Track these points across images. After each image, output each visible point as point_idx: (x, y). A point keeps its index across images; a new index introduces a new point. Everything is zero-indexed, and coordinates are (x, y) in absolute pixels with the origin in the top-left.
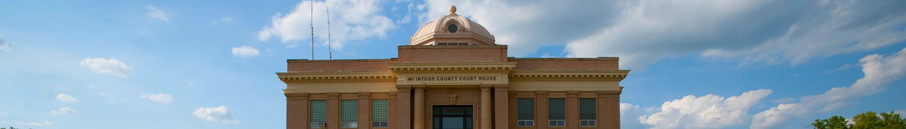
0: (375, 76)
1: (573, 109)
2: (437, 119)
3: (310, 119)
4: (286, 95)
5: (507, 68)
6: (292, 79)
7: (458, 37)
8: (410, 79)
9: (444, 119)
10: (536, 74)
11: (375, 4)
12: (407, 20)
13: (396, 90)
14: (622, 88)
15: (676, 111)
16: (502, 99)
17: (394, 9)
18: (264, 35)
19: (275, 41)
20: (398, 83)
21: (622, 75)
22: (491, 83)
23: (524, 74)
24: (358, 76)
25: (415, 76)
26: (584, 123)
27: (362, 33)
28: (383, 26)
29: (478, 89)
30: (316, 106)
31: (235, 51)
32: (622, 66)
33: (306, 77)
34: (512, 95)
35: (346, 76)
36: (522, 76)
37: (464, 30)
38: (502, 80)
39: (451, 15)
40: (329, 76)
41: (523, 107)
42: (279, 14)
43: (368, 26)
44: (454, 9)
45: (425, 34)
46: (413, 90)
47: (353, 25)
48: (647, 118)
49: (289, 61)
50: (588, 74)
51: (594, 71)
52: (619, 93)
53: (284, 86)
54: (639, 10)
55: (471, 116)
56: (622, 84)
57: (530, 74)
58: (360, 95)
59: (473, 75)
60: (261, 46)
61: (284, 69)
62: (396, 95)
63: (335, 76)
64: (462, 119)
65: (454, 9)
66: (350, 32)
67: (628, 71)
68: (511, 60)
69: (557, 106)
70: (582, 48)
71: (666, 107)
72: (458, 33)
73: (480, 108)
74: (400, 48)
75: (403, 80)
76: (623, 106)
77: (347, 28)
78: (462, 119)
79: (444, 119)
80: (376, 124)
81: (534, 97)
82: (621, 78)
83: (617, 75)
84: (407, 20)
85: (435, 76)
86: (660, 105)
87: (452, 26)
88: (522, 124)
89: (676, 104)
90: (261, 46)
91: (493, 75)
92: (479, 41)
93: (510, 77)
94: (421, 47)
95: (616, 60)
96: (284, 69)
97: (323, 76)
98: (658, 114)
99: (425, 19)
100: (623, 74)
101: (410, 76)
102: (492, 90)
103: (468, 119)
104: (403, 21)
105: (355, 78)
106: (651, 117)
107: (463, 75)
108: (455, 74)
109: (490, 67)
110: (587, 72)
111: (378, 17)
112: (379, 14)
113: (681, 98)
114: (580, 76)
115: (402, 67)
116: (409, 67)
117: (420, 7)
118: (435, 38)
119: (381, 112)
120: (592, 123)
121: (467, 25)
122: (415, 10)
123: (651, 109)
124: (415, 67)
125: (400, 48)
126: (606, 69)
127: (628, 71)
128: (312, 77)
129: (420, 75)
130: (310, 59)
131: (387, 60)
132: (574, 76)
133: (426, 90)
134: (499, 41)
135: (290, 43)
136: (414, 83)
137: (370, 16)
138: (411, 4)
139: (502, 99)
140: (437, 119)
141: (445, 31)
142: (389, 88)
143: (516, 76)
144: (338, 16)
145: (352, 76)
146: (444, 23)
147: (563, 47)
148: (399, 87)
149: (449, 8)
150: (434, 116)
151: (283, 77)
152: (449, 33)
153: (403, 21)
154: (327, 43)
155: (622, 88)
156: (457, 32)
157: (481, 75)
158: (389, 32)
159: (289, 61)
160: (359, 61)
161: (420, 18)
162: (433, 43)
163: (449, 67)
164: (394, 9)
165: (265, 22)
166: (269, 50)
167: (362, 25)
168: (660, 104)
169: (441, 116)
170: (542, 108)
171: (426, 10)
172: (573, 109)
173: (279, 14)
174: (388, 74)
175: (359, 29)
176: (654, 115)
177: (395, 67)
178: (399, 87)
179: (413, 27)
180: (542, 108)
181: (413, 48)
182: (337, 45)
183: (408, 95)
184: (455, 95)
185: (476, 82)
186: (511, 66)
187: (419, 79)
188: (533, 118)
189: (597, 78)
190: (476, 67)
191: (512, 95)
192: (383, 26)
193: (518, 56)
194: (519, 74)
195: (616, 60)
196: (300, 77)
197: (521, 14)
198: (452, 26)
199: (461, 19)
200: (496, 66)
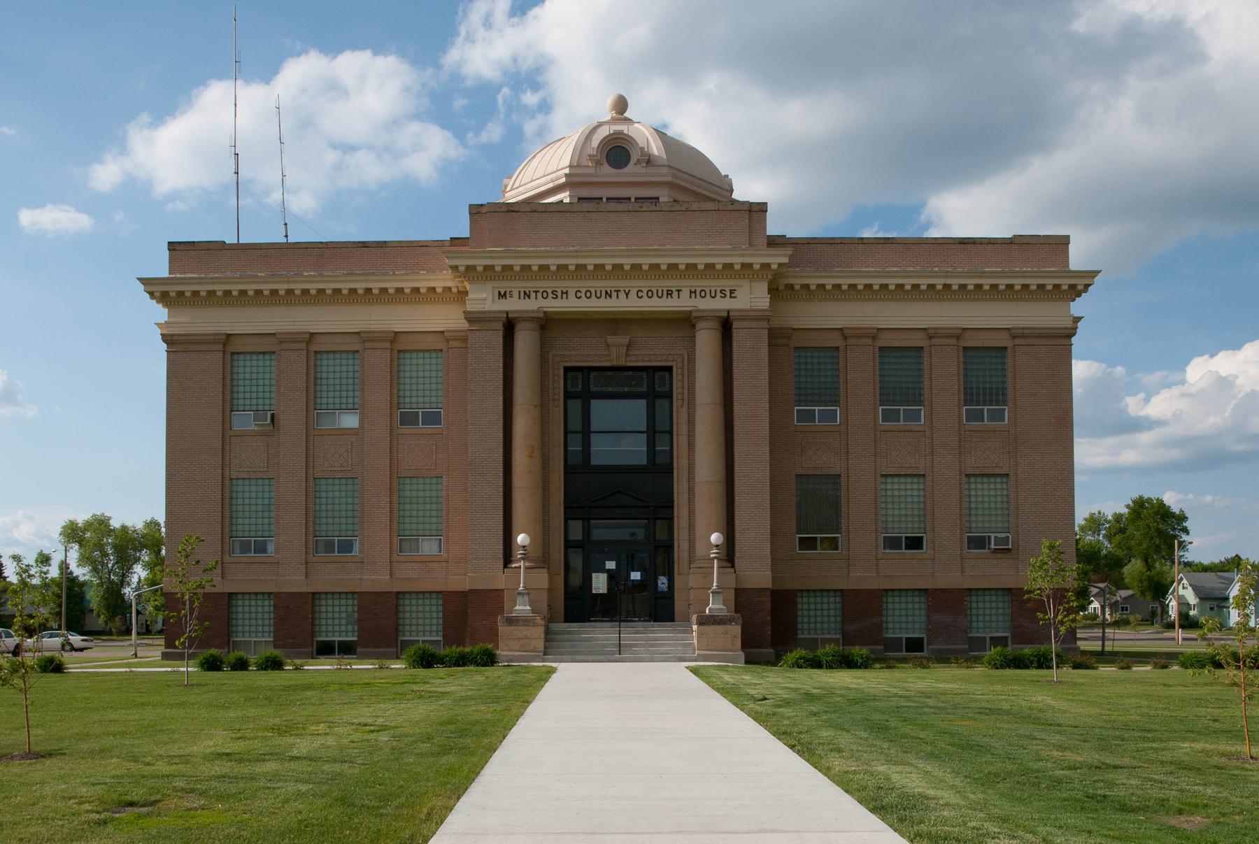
0: (407, 286)
1: (944, 377)
2: (576, 405)
3: (229, 406)
4: (165, 338)
5: (765, 266)
6: (181, 294)
7: (632, 181)
8: (502, 296)
9: (595, 404)
10: (845, 282)
11: (407, 89)
12: (494, 132)
13: (464, 325)
14: (1077, 320)
15: (1224, 383)
16: (751, 352)
17: (459, 103)
18: (106, 175)
19: (136, 192)
20: (470, 308)
21: (1078, 285)
22: (722, 304)
23: (813, 282)
24: (361, 286)
25: (516, 286)
26: (976, 416)
27: (370, 170)
28: (429, 151)
29: (686, 322)
30: (247, 368)
31: (26, 217)
32: (1078, 258)
33: (219, 288)
34: (778, 338)
35: (329, 287)
36: (806, 287)
37: (649, 161)
38: (751, 297)
39: (613, 121)
40: (282, 287)
41: (807, 370)
42: (145, 118)
43: (389, 151)
44: (621, 105)
45: (541, 171)
46: (510, 326)
47: (348, 148)
48: (1147, 401)
49: (173, 246)
50: (986, 283)
51: (1001, 275)
52: (1069, 333)
53: (160, 313)
54: (1126, 107)
55: (669, 395)
56: (1077, 307)
57: (829, 283)
58: (366, 338)
59: (672, 284)
60: (95, 204)
61: (160, 268)
62: (463, 338)
63: (298, 287)
64: (642, 403)
65: (621, 105)
66: (338, 167)
67: (1095, 273)
68: (776, 242)
69: (902, 369)
70: (969, 210)
71: (1198, 371)
72: (632, 171)
73: (692, 374)
74: (476, 211)
75: (483, 298)
76: (1081, 370)
77: (332, 157)
78: (642, 403)
79: (595, 404)
80: (409, 419)
81: (839, 343)
82: (1075, 292)
83: (1065, 283)
84: (494, 132)
85: (571, 285)
86: (1182, 365)
87: (617, 151)
88: (809, 416)
89: (1224, 363)
90: (95, 204)
91: (728, 284)
92: (691, 190)
93: (773, 291)
94: (532, 208)
95: (1061, 244)
96: (160, 268)
97: (266, 288)
98: (1176, 390)
99: (542, 131)
100: (1080, 282)
101: (503, 286)
102: (726, 325)
103: (661, 404)
104: (484, 137)
105: (353, 291)
106: (1156, 400)
107: (645, 284)
108: (626, 282)
109: (719, 261)
110: (982, 275)
111: (415, 127)
112: (416, 117)
113: (1237, 346)
114: (963, 287)
115: (480, 263)
116: (498, 263)
117: (530, 99)
118: (571, 183)
119: (425, 384)
120: (998, 416)
121: (656, 148)
122: (515, 107)
123: (1156, 377)
124: (517, 263)
125: (476, 211)
126: (1036, 268)
127: (1095, 273)
128: (235, 288)
129: (530, 285)
130: (231, 239)
131: (439, 244)
132: (947, 287)
133: (546, 324)
134: (745, 190)
135: (174, 196)
136: (514, 305)
137: (395, 123)
138: (506, 91)
139: (751, 352)
140: (576, 405)
141: (598, 163)
142: (445, 318)
143: (790, 287)
144: (307, 123)
145: (345, 287)
146: (595, 142)
147: (918, 208)
148: (472, 318)
149: (609, 101)
150: (568, 396)
151: (157, 290)
152: (607, 169)
153: (484, 137)
154: (276, 196)
155: (1077, 320)
156: (630, 168)
157: (696, 284)
158: (445, 167)
159: (173, 246)
160: (364, 245)
161: (530, 127)
162: (565, 197)
163: (609, 262)
164: (459, 103)
165: (109, 138)
166: (119, 217)
167: (371, 148)
168: (1181, 364)
169: (586, 397)
170: (860, 375)
171: (545, 107)
172: (944, 377)
173: (145, 118)
174: (443, 280)
175: (363, 157)
176: (1165, 394)
177: (462, 263)
178: (472, 318)
179: (511, 152)
180: (860, 375)
181: (511, 210)
182: (303, 203)
183: (498, 339)
184: (624, 340)
185: (682, 303)
186: (777, 259)
187: (527, 295)
188: (836, 402)
189: (1010, 293)
190: (682, 261)
191: (778, 338)
192: (429, 151)
193: (793, 232)
194: (797, 283)
195: (1061, 244)
196: (203, 289)
197: (809, 115)
198: (617, 151)
199: (642, 132)
200: (737, 261)
